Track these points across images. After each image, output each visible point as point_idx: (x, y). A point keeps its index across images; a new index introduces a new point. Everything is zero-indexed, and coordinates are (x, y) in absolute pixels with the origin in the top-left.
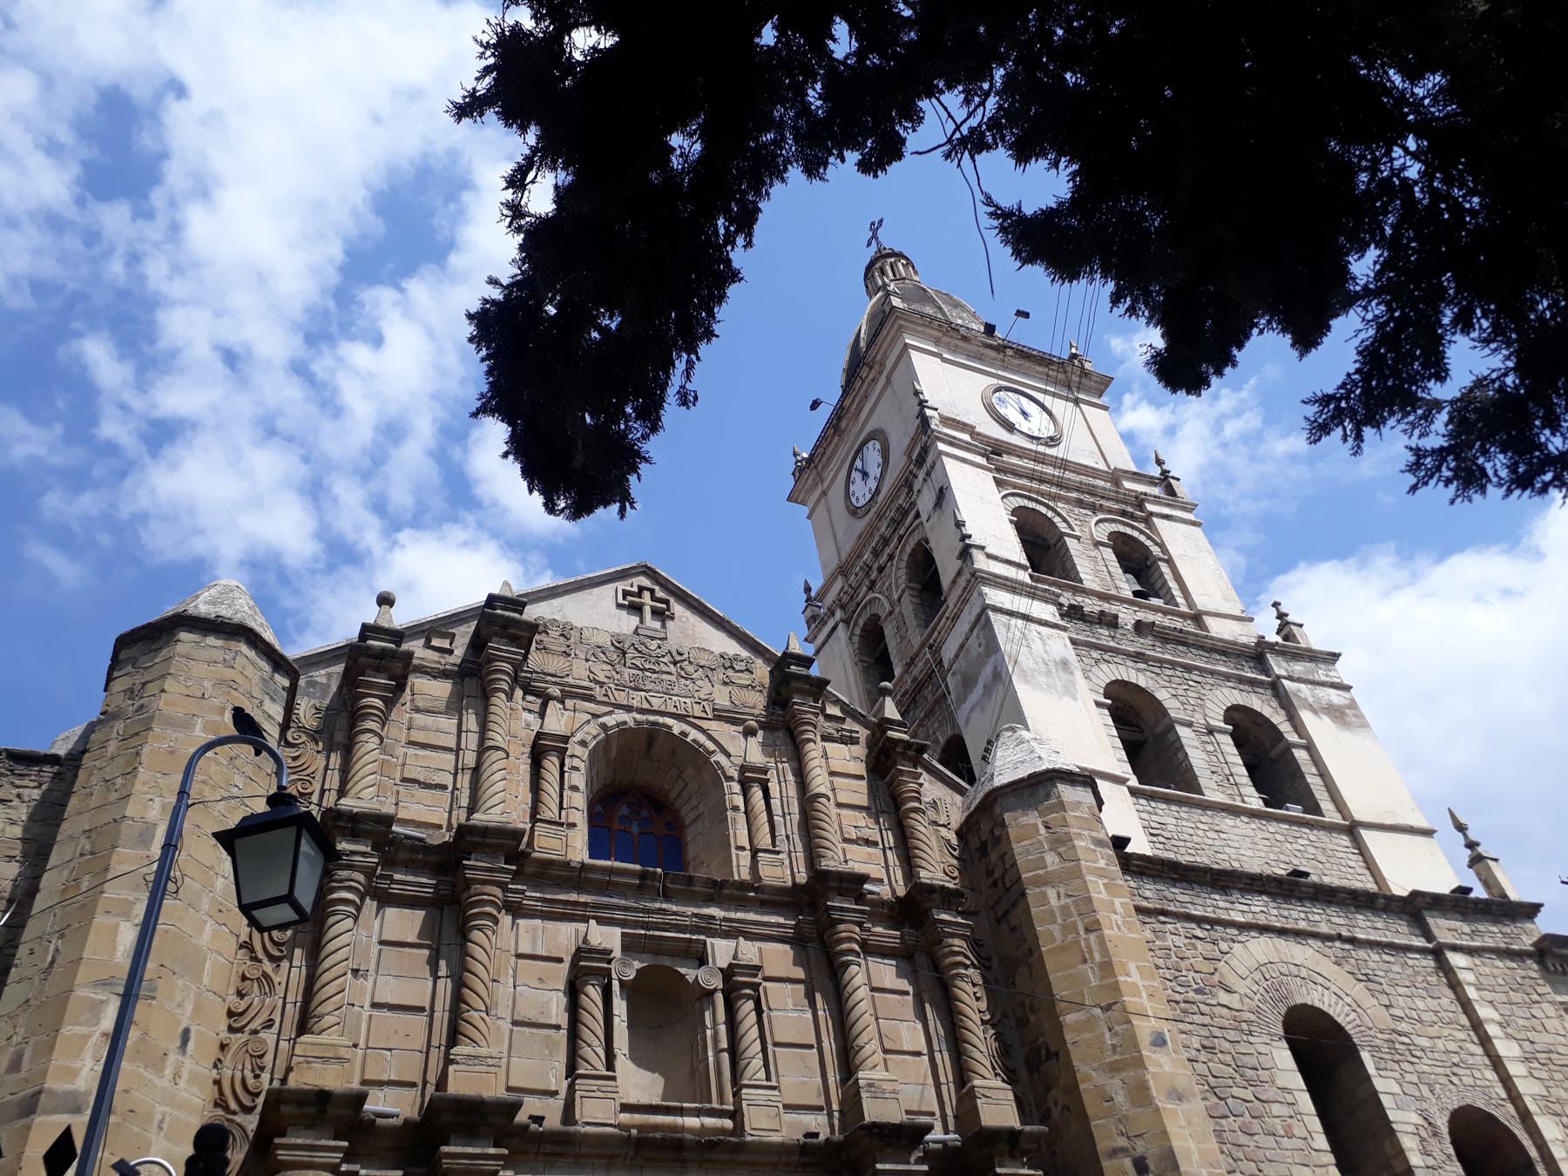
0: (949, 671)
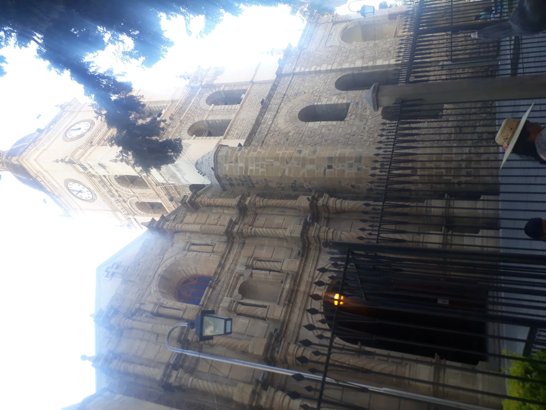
0: (167, 182)
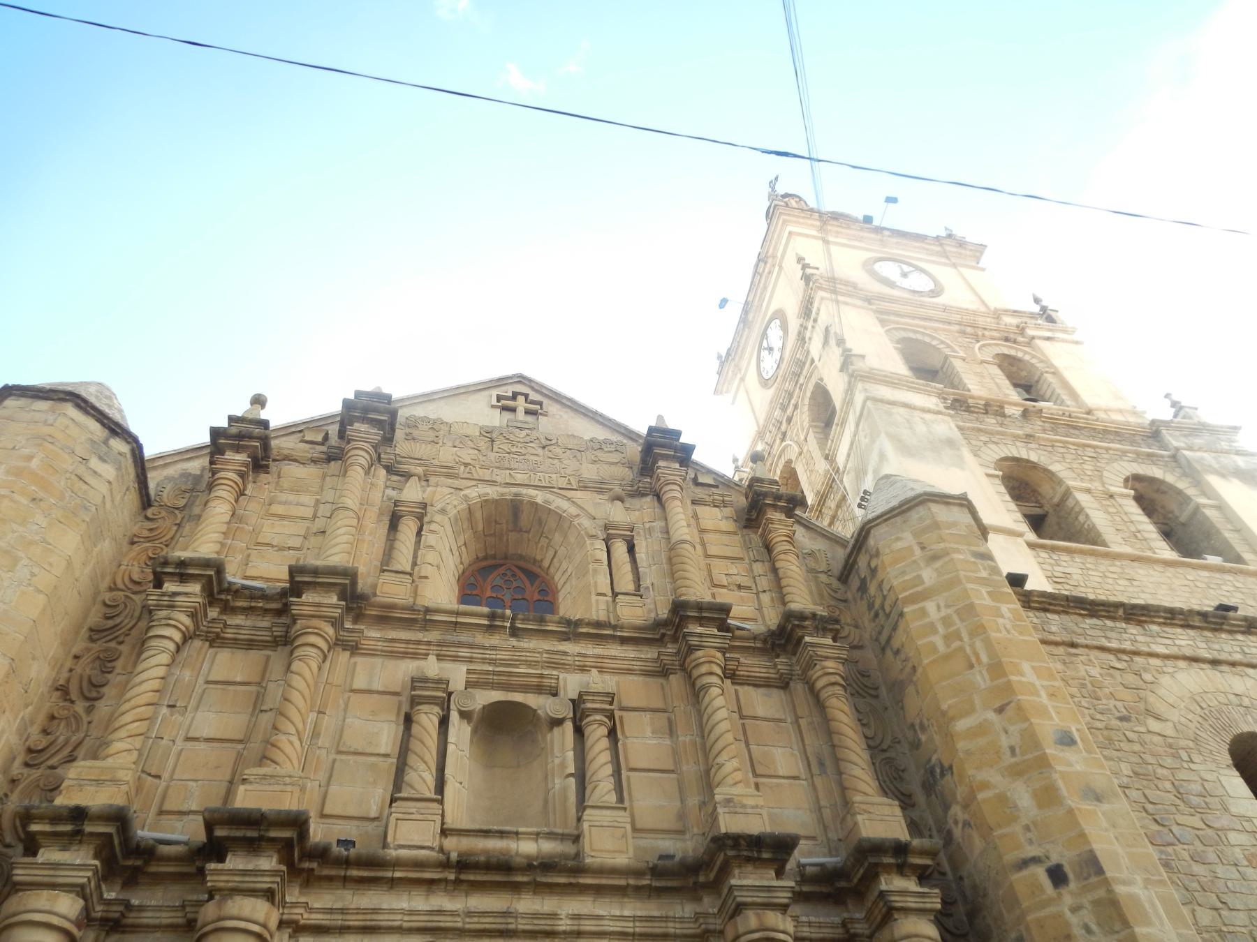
0: (844, 472)
